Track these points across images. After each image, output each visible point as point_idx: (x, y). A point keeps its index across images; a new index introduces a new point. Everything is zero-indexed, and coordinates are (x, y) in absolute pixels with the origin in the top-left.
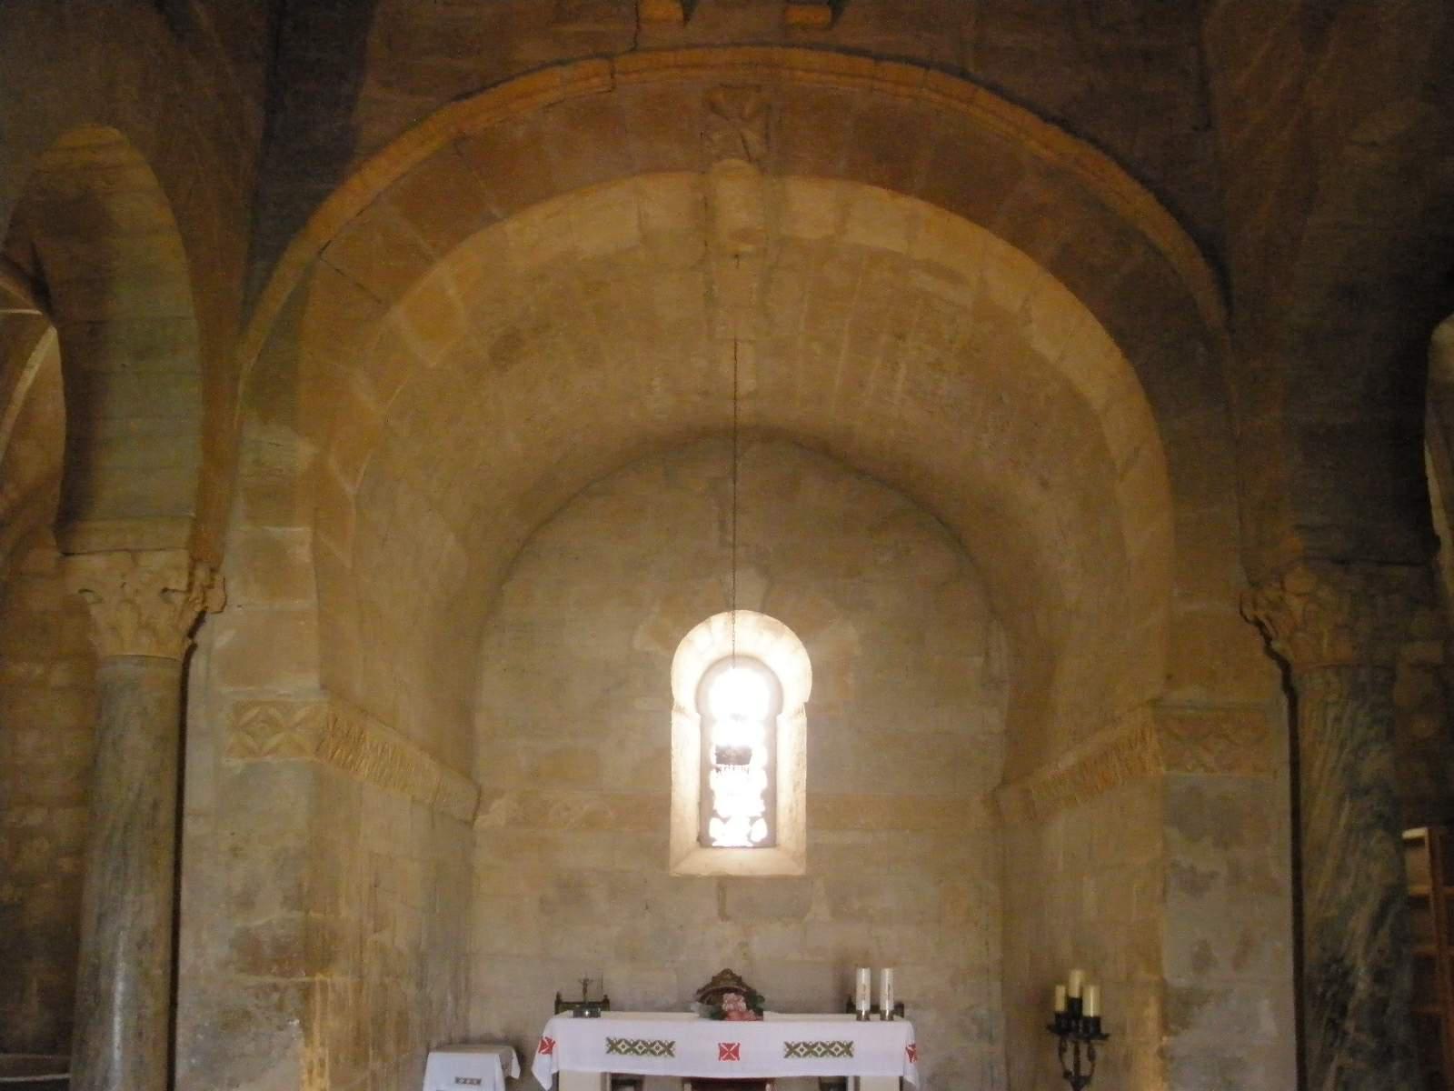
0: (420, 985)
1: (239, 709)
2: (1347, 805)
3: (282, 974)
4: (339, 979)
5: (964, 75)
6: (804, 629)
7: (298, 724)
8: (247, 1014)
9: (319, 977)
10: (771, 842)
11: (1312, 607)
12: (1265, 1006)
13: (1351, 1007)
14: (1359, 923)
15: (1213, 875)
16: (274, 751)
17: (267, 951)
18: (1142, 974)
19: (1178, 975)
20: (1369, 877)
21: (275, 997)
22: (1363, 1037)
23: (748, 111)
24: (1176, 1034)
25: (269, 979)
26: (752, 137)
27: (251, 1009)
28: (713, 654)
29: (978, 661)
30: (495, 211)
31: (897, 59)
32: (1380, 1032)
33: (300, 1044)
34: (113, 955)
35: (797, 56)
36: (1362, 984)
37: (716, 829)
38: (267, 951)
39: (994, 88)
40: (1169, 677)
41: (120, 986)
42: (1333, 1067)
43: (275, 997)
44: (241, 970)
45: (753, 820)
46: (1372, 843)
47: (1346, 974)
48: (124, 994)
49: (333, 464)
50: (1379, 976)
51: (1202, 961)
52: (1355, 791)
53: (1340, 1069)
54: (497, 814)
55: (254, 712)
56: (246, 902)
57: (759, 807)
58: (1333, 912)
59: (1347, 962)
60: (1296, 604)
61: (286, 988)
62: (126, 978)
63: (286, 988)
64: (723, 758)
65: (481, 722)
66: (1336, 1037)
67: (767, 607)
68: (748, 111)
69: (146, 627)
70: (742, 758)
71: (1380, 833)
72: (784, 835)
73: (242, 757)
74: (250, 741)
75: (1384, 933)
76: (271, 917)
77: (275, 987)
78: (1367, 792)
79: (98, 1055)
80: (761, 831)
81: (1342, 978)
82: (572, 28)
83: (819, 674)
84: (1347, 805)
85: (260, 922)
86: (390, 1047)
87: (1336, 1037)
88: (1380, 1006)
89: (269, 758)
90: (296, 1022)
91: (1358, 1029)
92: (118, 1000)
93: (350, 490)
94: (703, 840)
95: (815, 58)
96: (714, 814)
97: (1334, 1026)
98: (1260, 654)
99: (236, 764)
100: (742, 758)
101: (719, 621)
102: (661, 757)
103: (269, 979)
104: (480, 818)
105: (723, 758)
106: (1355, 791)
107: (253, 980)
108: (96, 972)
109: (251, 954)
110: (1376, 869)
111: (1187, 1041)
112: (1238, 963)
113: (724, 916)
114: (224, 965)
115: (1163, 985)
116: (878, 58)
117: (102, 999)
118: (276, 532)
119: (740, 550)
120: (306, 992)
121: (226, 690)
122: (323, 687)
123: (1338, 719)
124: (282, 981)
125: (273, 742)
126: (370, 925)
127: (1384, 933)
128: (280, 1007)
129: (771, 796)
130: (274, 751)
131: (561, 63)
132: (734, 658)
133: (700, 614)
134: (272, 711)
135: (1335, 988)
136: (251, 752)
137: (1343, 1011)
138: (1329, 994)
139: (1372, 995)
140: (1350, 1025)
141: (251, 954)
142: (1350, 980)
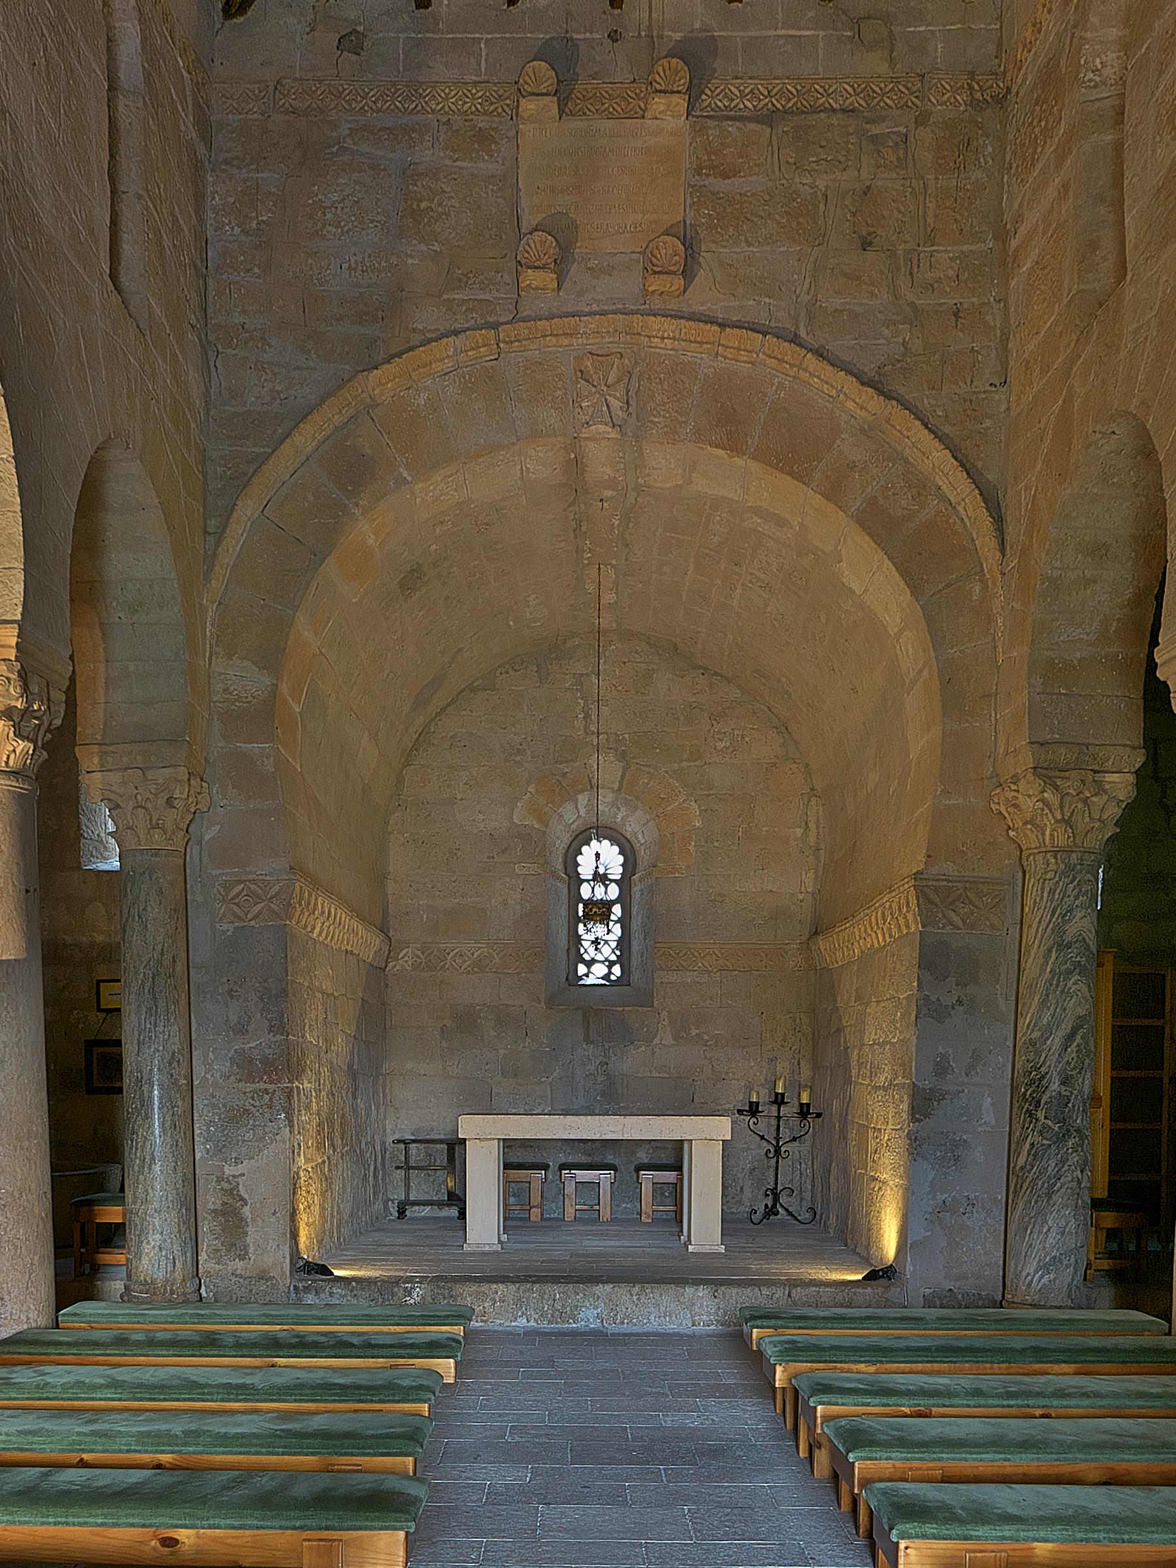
1: (227, 887)
5: (795, 340)
7: (272, 897)
14: (1056, 1041)
31: (737, 326)
36: (1055, 1086)
39: (820, 353)
40: (929, 856)
46: (1070, 984)
53: (1032, 1144)
66: (1031, 1122)
73: (233, 922)
74: (236, 908)
78: (1068, 946)
81: (1039, 1083)
87: (1031, 1122)
89: (252, 923)
91: (1046, 1118)
95: (670, 327)
97: (1030, 1114)
99: (228, 927)
106: (1063, 946)
107: (250, 1087)
116: (723, 325)
117: (146, 1103)
123: (1052, 892)
131: (456, 333)
134: (253, 887)
135: (1034, 1087)
136: (239, 918)
138: (1028, 1093)
140: (1041, 1114)
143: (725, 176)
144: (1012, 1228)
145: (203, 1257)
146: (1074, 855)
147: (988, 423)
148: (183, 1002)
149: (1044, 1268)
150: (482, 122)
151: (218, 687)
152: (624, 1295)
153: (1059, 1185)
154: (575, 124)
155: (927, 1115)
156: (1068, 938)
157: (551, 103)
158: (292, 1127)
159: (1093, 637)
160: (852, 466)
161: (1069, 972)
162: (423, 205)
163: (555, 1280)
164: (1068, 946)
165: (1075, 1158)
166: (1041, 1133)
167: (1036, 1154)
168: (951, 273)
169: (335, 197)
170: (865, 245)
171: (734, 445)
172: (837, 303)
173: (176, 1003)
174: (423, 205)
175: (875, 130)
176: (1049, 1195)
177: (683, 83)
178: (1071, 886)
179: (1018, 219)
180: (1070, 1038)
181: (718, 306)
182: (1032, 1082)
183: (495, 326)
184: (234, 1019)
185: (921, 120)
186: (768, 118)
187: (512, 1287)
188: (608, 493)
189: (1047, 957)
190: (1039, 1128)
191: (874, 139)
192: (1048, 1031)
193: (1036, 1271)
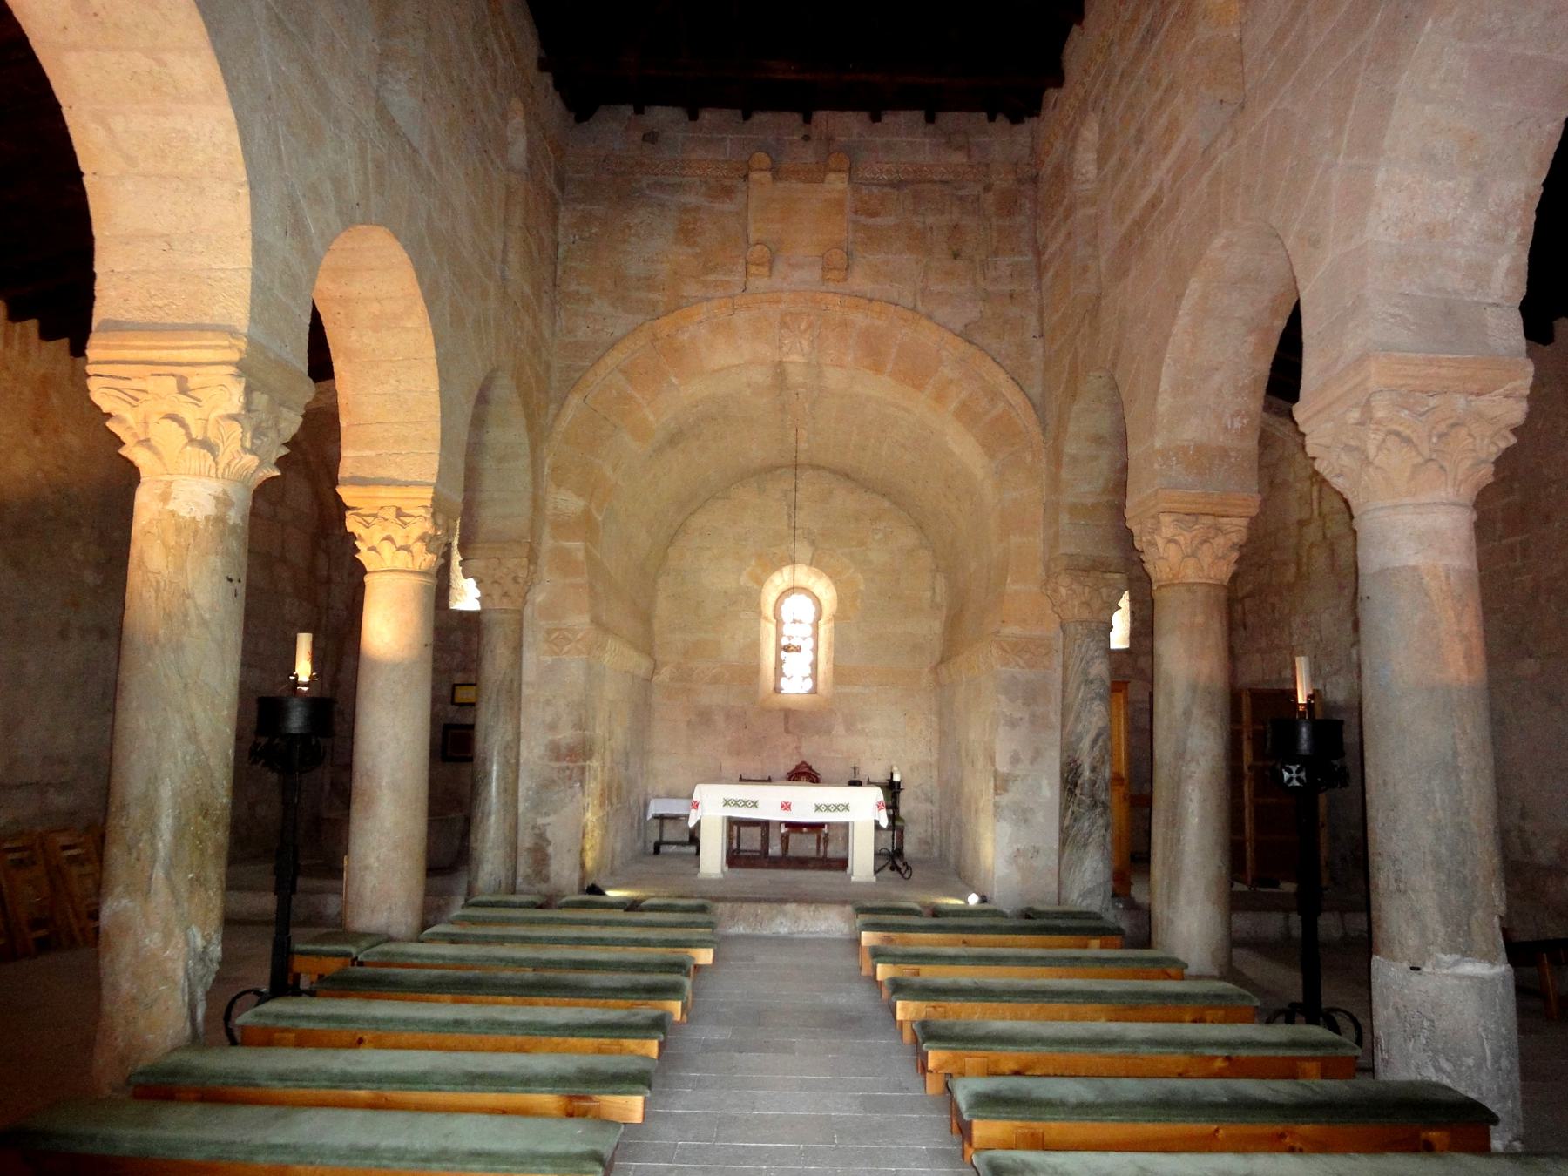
0: (627, 768)
1: (549, 632)
2: (1082, 686)
3: (571, 761)
4: (595, 763)
6: (834, 576)
7: (579, 640)
8: (553, 782)
9: (588, 763)
10: (814, 691)
11: (1070, 592)
12: (1045, 782)
13: (1079, 783)
14: (1086, 744)
15: (1021, 719)
16: (567, 653)
17: (563, 750)
18: (989, 767)
19: (1003, 766)
20: (1090, 723)
21: (568, 772)
22: (1083, 798)
23: (802, 327)
24: (1000, 794)
25: (565, 764)
26: (805, 344)
27: (556, 778)
28: (783, 587)
29: (929, 594)
30: (674, 380)
32: (1093, 796)
33: (580, 795)
34: (492, 754)
35: (830, 297)
36: (1087, 774)
37: (784, 683)
38: (563, 750)
41: (495, 768)
42: (1070, 812)
43: (568, 772)
44: (551, 760)
45: (804, 678)
46: (1093, 706)
47: (1078, 767)
48: (498, 771)
49: (593, 506)
50: (1093, 770)
51: (1015, 760)
52: (1089, 682)
53: (1073, 812)
54: (664, 675)
55: (557, 633)
56: (553, 727)
57: (808, 671)
58: (1073, 739)
59: (1079, 762)
60: (1063, 591)
61: (573, 768)
62: (498, 763)
63: (573, 768)
64: (787, 649)
65: (656, 626)
67: (816, 563)
68: (802, 327)
69: (505, 594)
70: (798, 650)
71: (1097, 702)
72: (821, 687)
74: (555, 648)
75: (1097, 749)
76: (566, 735)
77: (568, 768)
79: (486, 799)
80: (809, 684)
82: (711, 277)
83: (840, 601)
84: (1082, 686)
85: (560, 737)
86: (615, 800)
88: (1093, 783)
90: (578, 785)
92: (494, 775)
93: (600, 519)
94: (777, 690)
96: (783, 675)
97: (1071, 792)
98: (1050, 612)
99: (548, 659)
100: (798, 650)
101: (787, 570)
102: (755, 646)
103: (565, 764)
104: (655, 678)
105: (787, 649)
108: (484, 760)
109: (555, 752)
110: (1095, 719)
111: (1005, 799)
112: (1033, 761)
113: (787, 731)
114: (541, 758)
115: (996, 771)
118: (567, 544)
119: (799, 532)
120: (583, 770)
121: (543, 623)
122: (592, 621)
124: (571, 765)
125: (566, 649)
126: (607, 735)
127: (1097, 749)
128: (570, 778)
129: (814, 665)
130: (567, 653)
132: (793, 589)
133: (776, 566)
137: (1076, 785)
139: (1090, 779)
140: (1078, 792)
141: (555, 752)
142: (1079, 771)
143: (874, 214)
144: (1063, 868)
145: (519, 880)
146: (1093, 624)
147: (1033, 359)
148: (516, 708)
149: (1083, 895)
150: (727, 182)
151: (550, 506)
152: (805, 912)
153: (1090, 840)
154: (780, 185)
155: (1006, 790)
156: (1091, 677)
157: (768, 175)
158: (584, 792)
159: (1098, 490)
160: (951, 381)
161: (1093, 699)
162: (691, 226)
163: (759, 901)
164: (1092, 682)
165: (1101, 822)
166: (1079, 805)
167: (1075, 819)
168: (1008, 273)
169: (636, 221)
170: (956, 256)
171: (878, 368)
172: (940, 288)
173: (512, 708)
174: (691, 226)
175: (961, 193)
176: (1085, 846)
177: (846, 167)
178: (1091, 644)
179: (1045, 246)
180: (1095, 741)
181: (868, 287)
182: (1072, 770)
183: (731, 297)
184: (548, 719)
185: (987, 188)
186: (897, 185)
187: (729, 905)
188: (800, 390)
189: (1078, 689)
190: (1076, 802)
191: (961, 199)
192: (1080, 739)
193: (1078, 898)
